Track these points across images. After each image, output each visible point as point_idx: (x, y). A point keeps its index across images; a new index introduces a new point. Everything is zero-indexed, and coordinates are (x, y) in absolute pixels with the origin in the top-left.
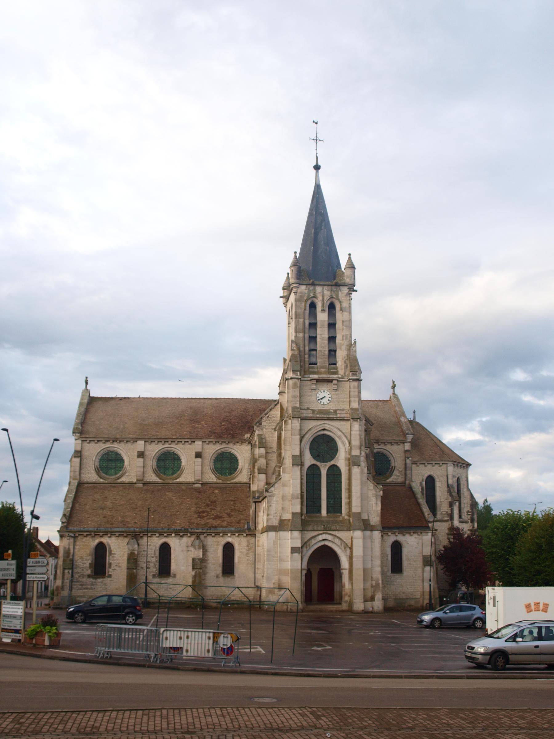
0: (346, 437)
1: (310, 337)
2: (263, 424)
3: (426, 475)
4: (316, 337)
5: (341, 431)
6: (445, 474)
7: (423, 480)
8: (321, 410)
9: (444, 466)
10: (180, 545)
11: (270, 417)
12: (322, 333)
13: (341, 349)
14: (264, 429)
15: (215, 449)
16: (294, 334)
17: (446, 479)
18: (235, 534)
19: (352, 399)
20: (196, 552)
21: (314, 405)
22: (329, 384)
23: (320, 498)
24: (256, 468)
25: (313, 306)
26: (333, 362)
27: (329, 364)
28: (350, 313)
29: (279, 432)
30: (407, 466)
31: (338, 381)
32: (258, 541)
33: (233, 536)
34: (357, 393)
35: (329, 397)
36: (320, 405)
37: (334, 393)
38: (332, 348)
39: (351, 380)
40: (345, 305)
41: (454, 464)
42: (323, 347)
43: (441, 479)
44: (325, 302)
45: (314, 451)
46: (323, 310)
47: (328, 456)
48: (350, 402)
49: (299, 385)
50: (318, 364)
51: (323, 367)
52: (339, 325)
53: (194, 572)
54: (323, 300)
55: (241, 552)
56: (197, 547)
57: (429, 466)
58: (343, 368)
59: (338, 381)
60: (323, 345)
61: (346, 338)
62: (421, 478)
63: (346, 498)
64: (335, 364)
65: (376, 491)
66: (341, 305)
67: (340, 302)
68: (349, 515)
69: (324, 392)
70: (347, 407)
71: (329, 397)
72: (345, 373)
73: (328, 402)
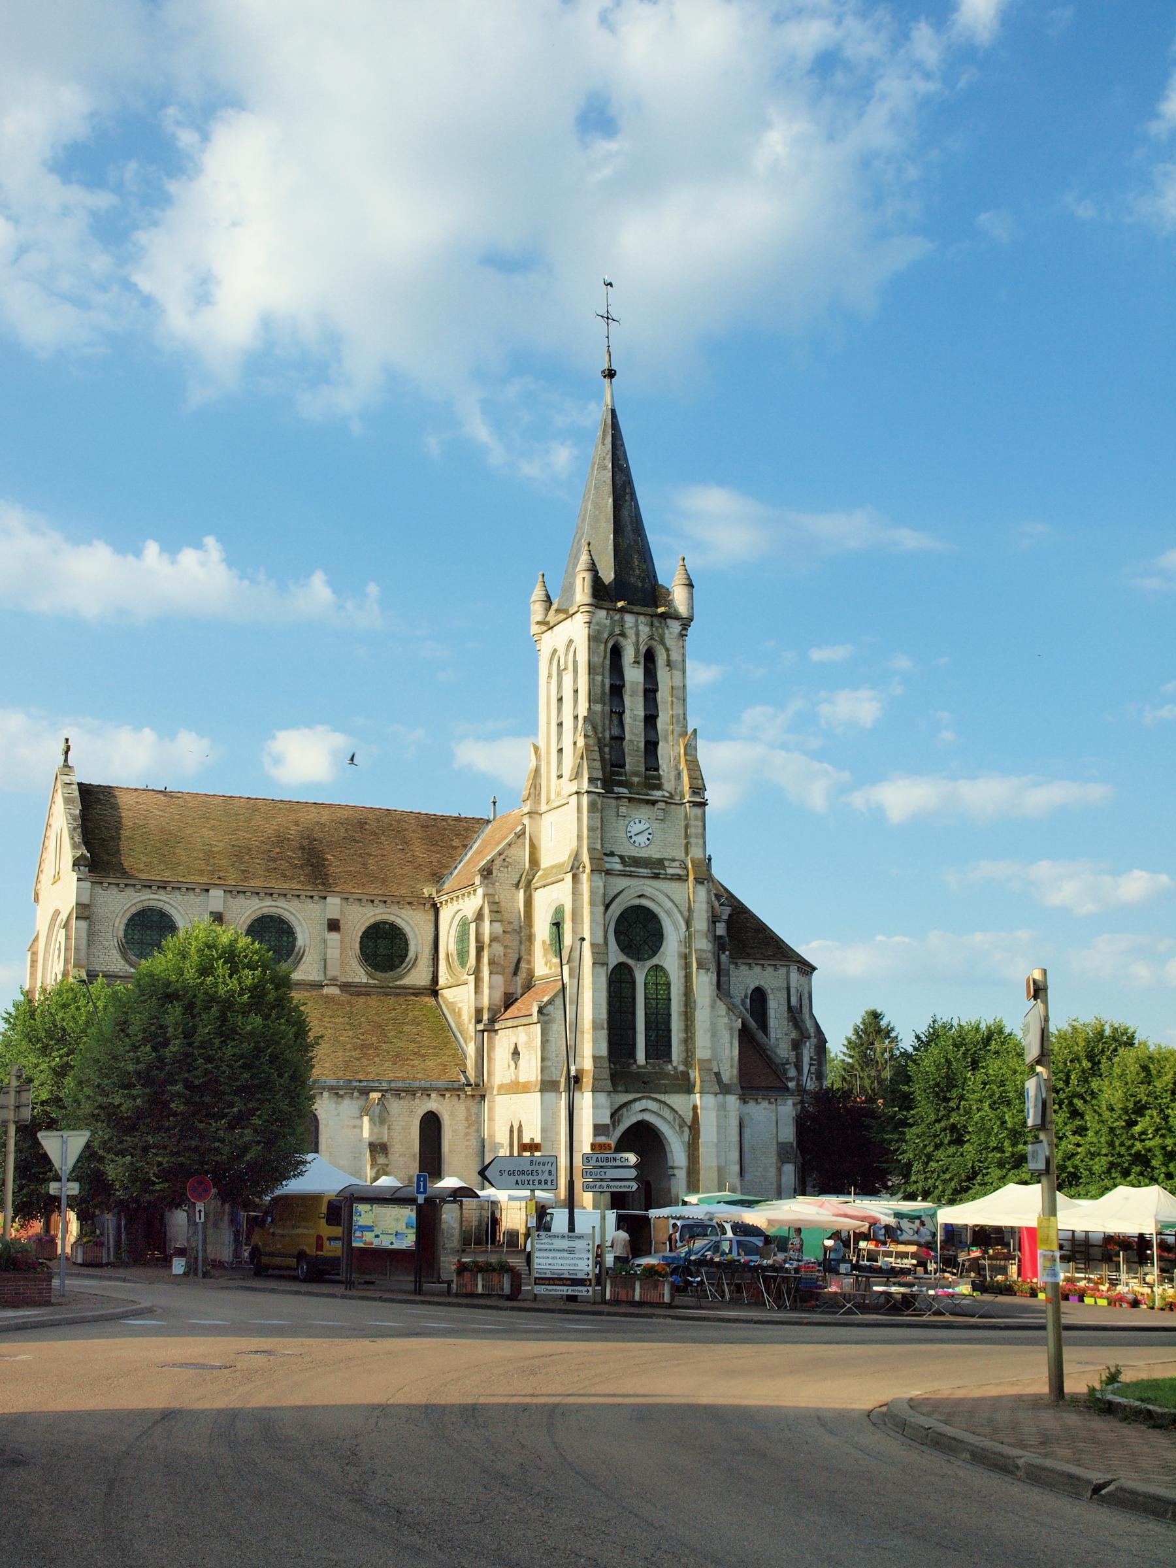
0: (682, 914)
1: (611, 711)
2: (494, 875)
3: (752, 987)
4: (624, 712)
6: (785, 985)
7: (746, 996)
8: (634, 857)
9: (783, 971)
10: (338, 1115)
11: (507, 860)
12: (634, 708)
14: (497, 884)
15: (365, 914)
16: (587, 705)
17: (786, 996)
18: (444, 1095)
19: (693, 840)
20: (376, 1130)
21: (622, 847)
22: (649, 807)
23: (634, 1029)
24: (485, 960)
27: (647, 769)
29: (528, 893)
30: (722, 967)
31: (666, 802)
32: (491, 1110)
33: (441, 1099)
34: (700, 831)
35: (650, 834)
36: (633, 848)
37: (657, 825)
41: (798, 967)
43: (778, 994)
45: (622, 937)
47: (646, 948)
48: (687, 845)
49: (599, 807)
50: (627, 767)
51: (636, 774)
52: (663, 695)
55: (454, 1131)
56: (377, 1119)
57: (757, 969)
58: (673, 779)
59: (666, 802)
60: (636, 731)
61: (678, 722)
62: (744, 992)
64: (657, 769)
65: (730, 1019)
69: (640, 822)
70: (681, 855)
71: (650, 834)
72: (676, 789)
73: (648, 842)
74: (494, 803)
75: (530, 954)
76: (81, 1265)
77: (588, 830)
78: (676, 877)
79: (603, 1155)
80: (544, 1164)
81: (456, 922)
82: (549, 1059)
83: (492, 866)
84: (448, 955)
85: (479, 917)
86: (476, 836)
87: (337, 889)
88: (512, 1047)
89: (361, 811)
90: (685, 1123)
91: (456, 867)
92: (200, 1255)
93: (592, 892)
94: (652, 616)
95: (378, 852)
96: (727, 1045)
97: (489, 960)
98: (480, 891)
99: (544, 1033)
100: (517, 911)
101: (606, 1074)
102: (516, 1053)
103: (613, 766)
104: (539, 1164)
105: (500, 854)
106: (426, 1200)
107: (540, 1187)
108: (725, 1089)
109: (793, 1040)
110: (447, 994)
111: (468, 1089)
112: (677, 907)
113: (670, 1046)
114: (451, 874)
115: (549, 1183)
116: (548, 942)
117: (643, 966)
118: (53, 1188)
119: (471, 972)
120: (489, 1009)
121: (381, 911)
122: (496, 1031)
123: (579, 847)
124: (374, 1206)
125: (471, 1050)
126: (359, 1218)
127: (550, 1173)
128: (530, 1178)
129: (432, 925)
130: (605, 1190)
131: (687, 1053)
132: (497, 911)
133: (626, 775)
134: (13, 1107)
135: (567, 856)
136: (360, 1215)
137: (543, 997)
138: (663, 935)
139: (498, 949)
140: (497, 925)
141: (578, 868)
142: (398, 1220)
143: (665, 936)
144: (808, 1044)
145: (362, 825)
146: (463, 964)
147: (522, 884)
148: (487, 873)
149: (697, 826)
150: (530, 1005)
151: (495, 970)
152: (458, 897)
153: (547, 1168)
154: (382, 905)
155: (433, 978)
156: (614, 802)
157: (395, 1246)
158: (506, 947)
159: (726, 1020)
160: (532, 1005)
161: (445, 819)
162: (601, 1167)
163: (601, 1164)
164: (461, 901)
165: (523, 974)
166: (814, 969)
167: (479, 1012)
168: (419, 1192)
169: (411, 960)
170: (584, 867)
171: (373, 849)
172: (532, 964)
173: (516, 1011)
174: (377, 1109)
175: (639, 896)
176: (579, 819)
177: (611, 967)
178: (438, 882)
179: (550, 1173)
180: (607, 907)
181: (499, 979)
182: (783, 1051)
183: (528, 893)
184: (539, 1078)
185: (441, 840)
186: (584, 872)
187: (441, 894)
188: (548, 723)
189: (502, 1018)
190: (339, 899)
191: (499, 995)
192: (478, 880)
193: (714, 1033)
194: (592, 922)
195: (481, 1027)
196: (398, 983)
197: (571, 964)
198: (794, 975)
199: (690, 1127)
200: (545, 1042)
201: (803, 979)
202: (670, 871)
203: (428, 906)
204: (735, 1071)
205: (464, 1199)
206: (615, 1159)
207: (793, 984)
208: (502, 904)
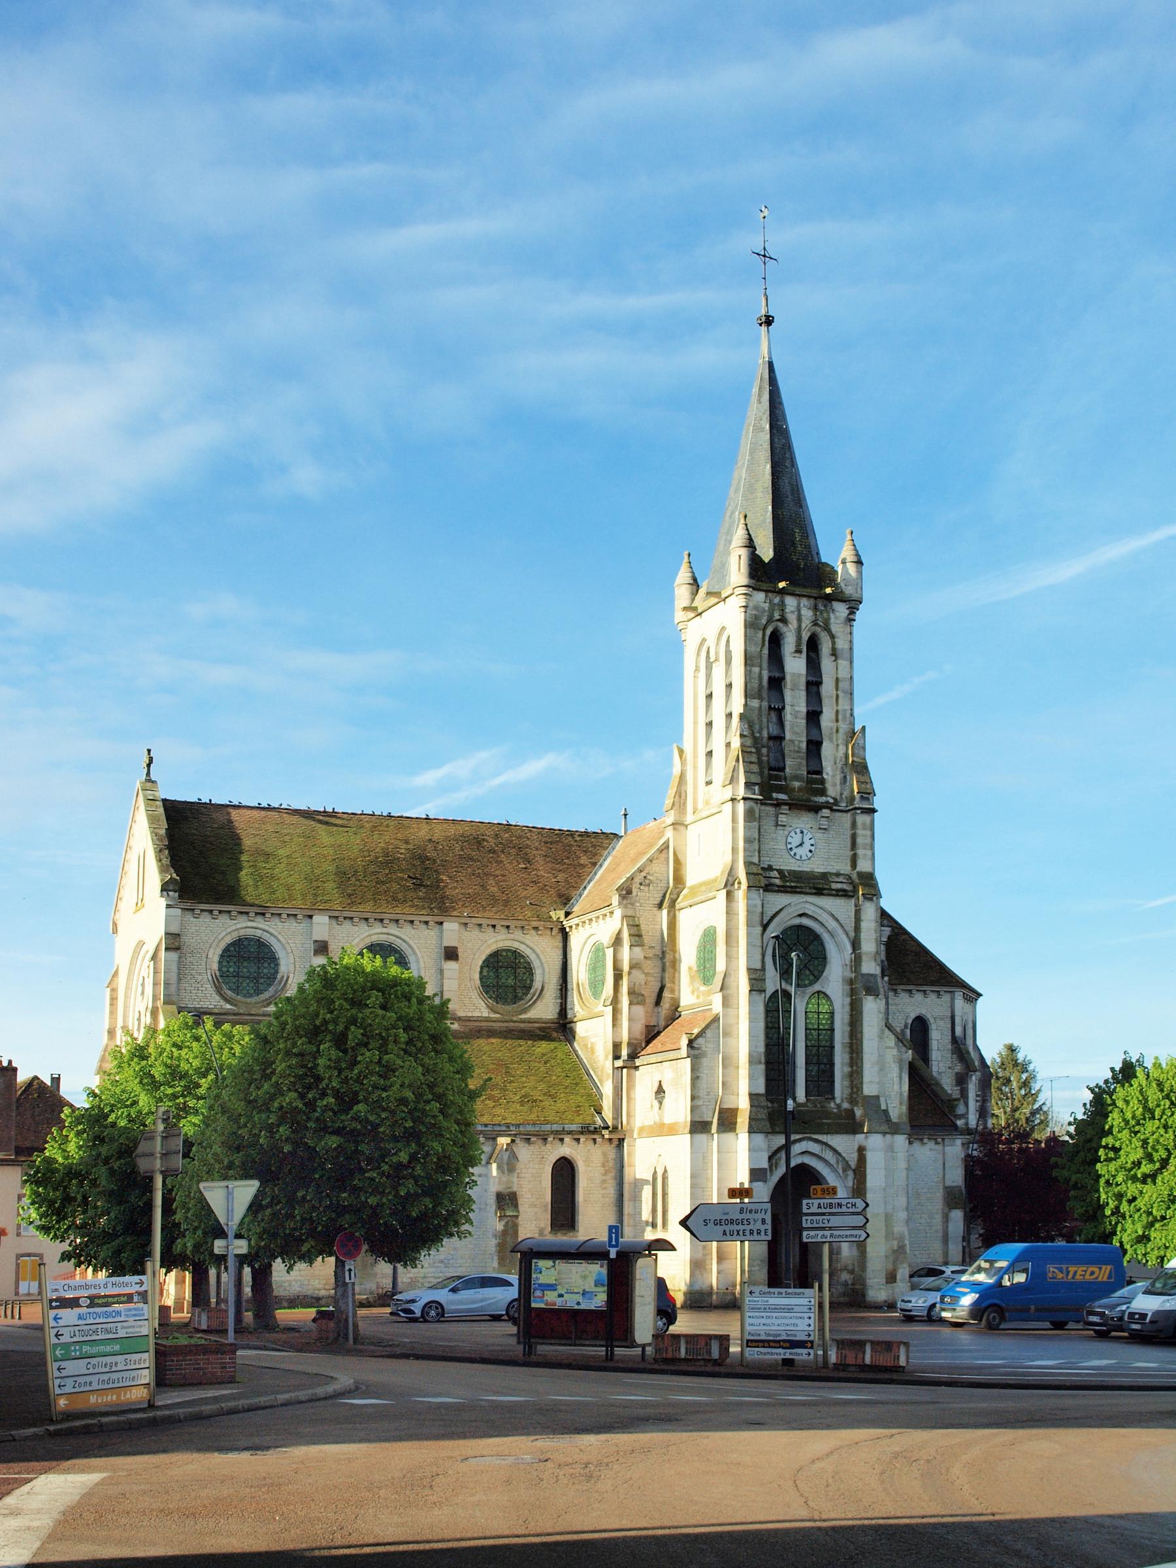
2: (634, 894)
5: (837, 920)
9: (946, 998)
13: (831, 740)
14: (638, 904)
21: (781, 860)
25: (775, 640)
26: (816, 769)
28: (851, 662)
29: (672, 914)
38: (815, 738)
39: (859, 811)
40: (841, 644)
42: (797, 733)
44: (803, 635)
46: (798, 651)
47: (807, 972)
53: (503, 1223)
54: (799, 630)
63: (843, 1064)
66: (834, 643)
67: (833, 637)
68: (852, 1100)
70: (845, 868)
74: (625, 815)
75: (673, 982)
76: (204, 1331)
77: (745, 842)
78: (840, 893)
79: (825, 1201)
80: (756, 1212)
81: (588, 947)
82: (699, 1098)
83: (631, 884)
84: (578, 984)
85: (617, 942)
86: (606, 852)
87: (455, 913)
88: (657, 1085)
89: (478, 826)
90: (849, 1166)
91: (585, 888)
92: (350, 1320)
93: (749, 912)
94: (816, 598)
95: (497, 872)
96: (896, 1080)
97: (629, 989)
98: (618, 913)
99: (694, 1069)
100: (659, 934)
101: (763, 1114)
102: (660, 1091)
103: (771, 769)
104: (751, 1211)
105: (641, 871)
106: (618, 1253)
107: (751, 1238)
108: (894, 1129)
109: (957, 1074)
110: (581, 1029)
111: (605, 1132)
112: (843, 927)
113: (833, 1081)
114: (580, 895)
115: (763, 1233)
116: (695, 968)
117: (804, 992)
118: (219, 1246)
119: (609, 1002)
120: (629, 1044)
121: (503, 937)
122: (637, 1068)
123: (734, 861)
124: (557, 1262)
125: (607, 1089)
126: (539, 1275)
127: (763, 1221)
128: (740, 1227)
129: (560, 952)
130: (828, 1240)
131: (852, 1089)
132: (637, 937)
133: (785, 779)
134: (159, 1155)
135: (719, 874)
136: (541, 1272)
137: (695, 1027)
138: (826, 958)
139: (639, 976)
140: (637, 950)
141: (733, 884)
142: (585, 1277)
143: (828, 959)
144: (974, 1078)
145: (478, 842)
146: (596, 994)
147: (666, 904)
148: (626, 892)
149: (865, 836)
150: (677, 1037)
151: (635, 1001)
152: (591, 920)
153: (760, 1216)
154: (504, 931)
155: (561, 1010)
156: (771, 810)
157: (583, 1307)
158: (647, 974)
159: (895, 1052)
160: (679, 1039)
161: (571, 834)
162: (824, 1214)
163: (823, 1210)
164: (594, 923)
165: (666, 1004)
166: (980, 995)
167: (617, 1046)
168: (611, 1246)
169: (536, 990)
170: (739, 883)
171: (493, 868)
172: (676, 993)
173: (660, 1045)
174: (506, 1156)
175: (800, 915)
176: (734, 830)
177: (769, 992)
178: (565, 904)
179: (763, 1221)
180: (765, 927)
181: (639, 1010)
182: (948, 1084)
183: (672, 914)
184: (689, 1119)
185: (568, 858)
186: (739, 888)
187: (570, 917)
188: (695, 723)
189: (642, 1053)
190: (457, 924)
191: (639, 1028)
192: (615, 900)
193: (881, 1065)
194: (749, 944)
195: (619, 1063)
196: (523, 1016)
197: (725, 992)
198: (959, 1003)
199: (854, 1170)
200: (695, 1079)
201: (968, 1007)
202: (834, 886)
203: (555, 931)
204: (904, 1108)
205: (659, 1253)
206: (840, 1205)
207: (958, 1013)
208: (643, 927)
